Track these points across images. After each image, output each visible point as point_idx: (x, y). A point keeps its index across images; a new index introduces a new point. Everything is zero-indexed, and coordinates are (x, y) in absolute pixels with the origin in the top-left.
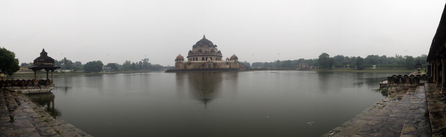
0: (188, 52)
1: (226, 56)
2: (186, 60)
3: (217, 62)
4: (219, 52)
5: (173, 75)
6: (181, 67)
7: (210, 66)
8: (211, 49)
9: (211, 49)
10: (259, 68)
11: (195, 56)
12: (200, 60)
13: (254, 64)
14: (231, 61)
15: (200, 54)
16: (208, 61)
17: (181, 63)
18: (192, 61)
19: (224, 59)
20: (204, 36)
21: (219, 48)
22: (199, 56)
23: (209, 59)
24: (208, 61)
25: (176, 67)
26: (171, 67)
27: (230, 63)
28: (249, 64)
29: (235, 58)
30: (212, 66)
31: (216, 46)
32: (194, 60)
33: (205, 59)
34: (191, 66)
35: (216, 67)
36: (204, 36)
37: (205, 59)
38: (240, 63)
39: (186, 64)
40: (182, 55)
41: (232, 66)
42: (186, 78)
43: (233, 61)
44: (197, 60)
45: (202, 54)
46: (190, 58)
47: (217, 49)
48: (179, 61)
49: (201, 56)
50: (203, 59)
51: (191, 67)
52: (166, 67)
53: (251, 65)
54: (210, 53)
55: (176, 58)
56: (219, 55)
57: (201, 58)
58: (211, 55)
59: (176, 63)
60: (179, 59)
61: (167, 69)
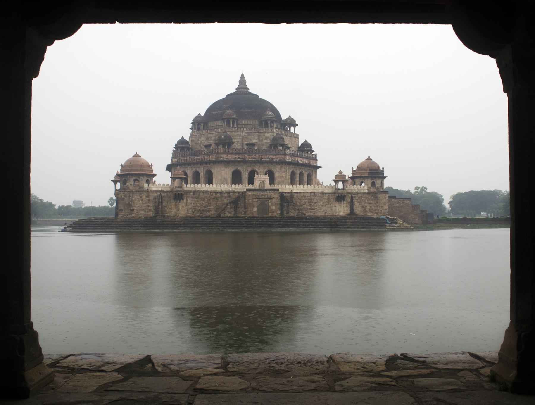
0: (172, 147)
1: (333, 164)
2: (163, 179)
3: (297, 188)
4: (306, 147)
5: (105, 244)
6: (142, 208)
7: (263, 205)
8: (270, 134)
9: (270, 134)
10: (483, 214)
11: (202, 163)
12: (224, 182)
13: (460, 200)
14: (355, 188)
15: (224, 157)
16: (257, 185)
17: (141, 191)
18: (190, 187)
19: (325, 177)
20: (242, 80)
21: (303, 133)
22: (218, 162)
23: (262, 179)
24: (257, 185)
25: (117, 210)
26: (91, 210)
27: (352, 195)
28: (437, 199)
29: (371, 173)
30: (274, 208)
31: (291, 123)
32: (196, 180)
33: (245, 176)
34: (182, 205)
35: (293, 214)
36: (242, 80)
37: (245, 176)
38: (395, 196)
39: (162, 198)
40: (147, 157)
41: (358, 209)
42: (161, 257)
43: (364, 187)
44: (210, 181)
45: (231, 157)
46: (180, 172)
47: (296, 137)
48: (130, 183)
49: (228, 163)
50: (236, 178)
51: (183, 209)
52: (65, 211)
53: (446, 204)
54: (266, 152)
55: (118, 169)
56: (304, 163)
57: (226, 172)
58: (271, 162)
59: (117, 193)
60: (133, 174)
61: (70, 220)
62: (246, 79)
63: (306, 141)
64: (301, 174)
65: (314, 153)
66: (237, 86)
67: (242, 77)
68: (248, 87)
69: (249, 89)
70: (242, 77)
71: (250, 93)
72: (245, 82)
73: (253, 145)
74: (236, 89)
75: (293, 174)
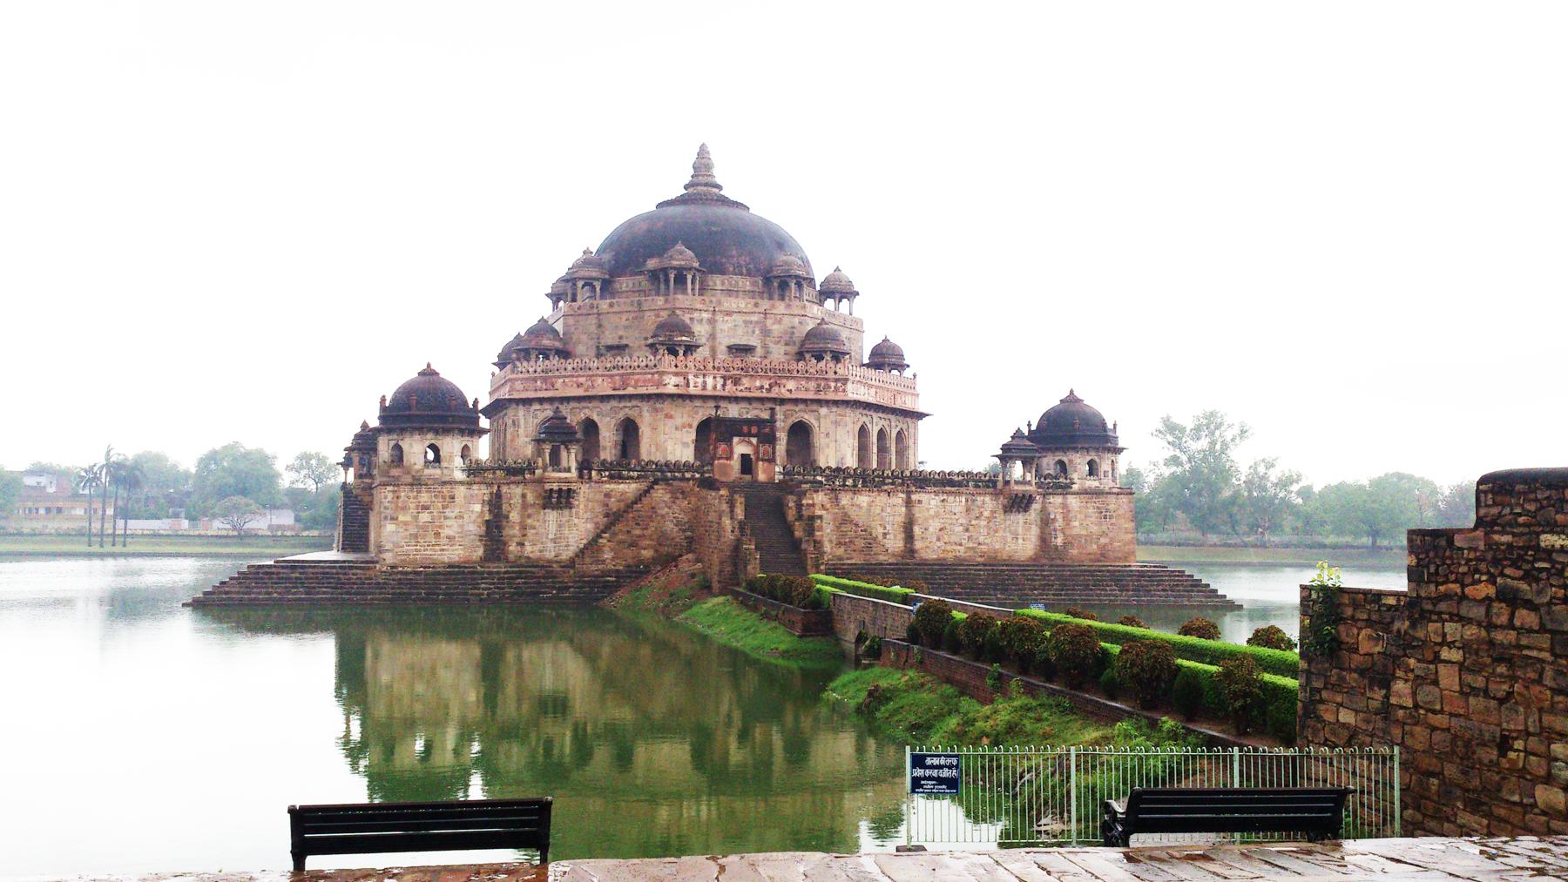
11: (604, 398)
20: (702, 165)
36: (702, 165)
47: (857, 327)
62: (715, 157)
63: (886, 340)
64: (882, 434)
65: (908, 373)
66: (688, 179)
67: (703, 153)
68: (718, 181)
69: (720, 187)
70: (703, 153)
71: (725, 201)
72: (708, 167)
73: (748, 349)
74: (686, 187)
75: (863, 432)
